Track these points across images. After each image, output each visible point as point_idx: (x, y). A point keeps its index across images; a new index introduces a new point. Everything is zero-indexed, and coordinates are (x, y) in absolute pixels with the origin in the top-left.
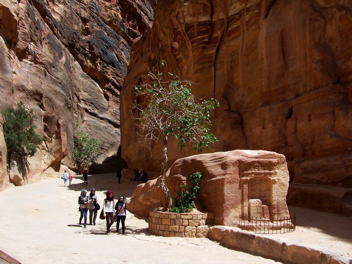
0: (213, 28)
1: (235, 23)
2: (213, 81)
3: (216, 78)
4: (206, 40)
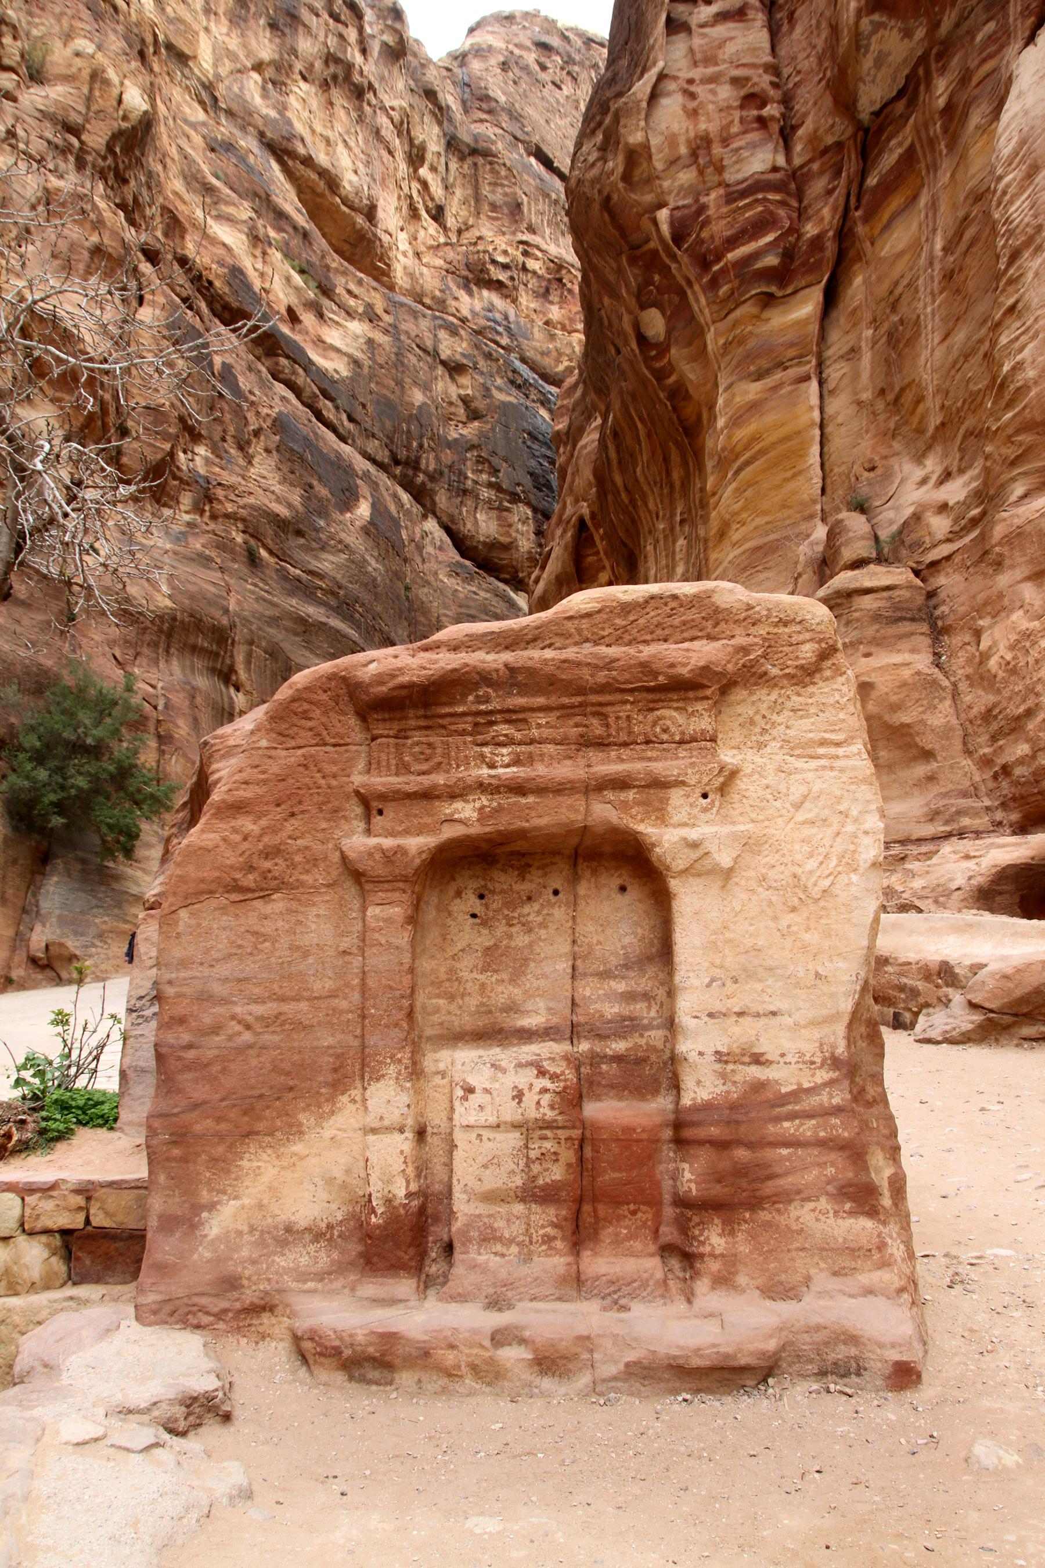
0: (800, 201)
1: (893, 142)
2: (815, 449)
3: (829, 429)
4: (771, 260)
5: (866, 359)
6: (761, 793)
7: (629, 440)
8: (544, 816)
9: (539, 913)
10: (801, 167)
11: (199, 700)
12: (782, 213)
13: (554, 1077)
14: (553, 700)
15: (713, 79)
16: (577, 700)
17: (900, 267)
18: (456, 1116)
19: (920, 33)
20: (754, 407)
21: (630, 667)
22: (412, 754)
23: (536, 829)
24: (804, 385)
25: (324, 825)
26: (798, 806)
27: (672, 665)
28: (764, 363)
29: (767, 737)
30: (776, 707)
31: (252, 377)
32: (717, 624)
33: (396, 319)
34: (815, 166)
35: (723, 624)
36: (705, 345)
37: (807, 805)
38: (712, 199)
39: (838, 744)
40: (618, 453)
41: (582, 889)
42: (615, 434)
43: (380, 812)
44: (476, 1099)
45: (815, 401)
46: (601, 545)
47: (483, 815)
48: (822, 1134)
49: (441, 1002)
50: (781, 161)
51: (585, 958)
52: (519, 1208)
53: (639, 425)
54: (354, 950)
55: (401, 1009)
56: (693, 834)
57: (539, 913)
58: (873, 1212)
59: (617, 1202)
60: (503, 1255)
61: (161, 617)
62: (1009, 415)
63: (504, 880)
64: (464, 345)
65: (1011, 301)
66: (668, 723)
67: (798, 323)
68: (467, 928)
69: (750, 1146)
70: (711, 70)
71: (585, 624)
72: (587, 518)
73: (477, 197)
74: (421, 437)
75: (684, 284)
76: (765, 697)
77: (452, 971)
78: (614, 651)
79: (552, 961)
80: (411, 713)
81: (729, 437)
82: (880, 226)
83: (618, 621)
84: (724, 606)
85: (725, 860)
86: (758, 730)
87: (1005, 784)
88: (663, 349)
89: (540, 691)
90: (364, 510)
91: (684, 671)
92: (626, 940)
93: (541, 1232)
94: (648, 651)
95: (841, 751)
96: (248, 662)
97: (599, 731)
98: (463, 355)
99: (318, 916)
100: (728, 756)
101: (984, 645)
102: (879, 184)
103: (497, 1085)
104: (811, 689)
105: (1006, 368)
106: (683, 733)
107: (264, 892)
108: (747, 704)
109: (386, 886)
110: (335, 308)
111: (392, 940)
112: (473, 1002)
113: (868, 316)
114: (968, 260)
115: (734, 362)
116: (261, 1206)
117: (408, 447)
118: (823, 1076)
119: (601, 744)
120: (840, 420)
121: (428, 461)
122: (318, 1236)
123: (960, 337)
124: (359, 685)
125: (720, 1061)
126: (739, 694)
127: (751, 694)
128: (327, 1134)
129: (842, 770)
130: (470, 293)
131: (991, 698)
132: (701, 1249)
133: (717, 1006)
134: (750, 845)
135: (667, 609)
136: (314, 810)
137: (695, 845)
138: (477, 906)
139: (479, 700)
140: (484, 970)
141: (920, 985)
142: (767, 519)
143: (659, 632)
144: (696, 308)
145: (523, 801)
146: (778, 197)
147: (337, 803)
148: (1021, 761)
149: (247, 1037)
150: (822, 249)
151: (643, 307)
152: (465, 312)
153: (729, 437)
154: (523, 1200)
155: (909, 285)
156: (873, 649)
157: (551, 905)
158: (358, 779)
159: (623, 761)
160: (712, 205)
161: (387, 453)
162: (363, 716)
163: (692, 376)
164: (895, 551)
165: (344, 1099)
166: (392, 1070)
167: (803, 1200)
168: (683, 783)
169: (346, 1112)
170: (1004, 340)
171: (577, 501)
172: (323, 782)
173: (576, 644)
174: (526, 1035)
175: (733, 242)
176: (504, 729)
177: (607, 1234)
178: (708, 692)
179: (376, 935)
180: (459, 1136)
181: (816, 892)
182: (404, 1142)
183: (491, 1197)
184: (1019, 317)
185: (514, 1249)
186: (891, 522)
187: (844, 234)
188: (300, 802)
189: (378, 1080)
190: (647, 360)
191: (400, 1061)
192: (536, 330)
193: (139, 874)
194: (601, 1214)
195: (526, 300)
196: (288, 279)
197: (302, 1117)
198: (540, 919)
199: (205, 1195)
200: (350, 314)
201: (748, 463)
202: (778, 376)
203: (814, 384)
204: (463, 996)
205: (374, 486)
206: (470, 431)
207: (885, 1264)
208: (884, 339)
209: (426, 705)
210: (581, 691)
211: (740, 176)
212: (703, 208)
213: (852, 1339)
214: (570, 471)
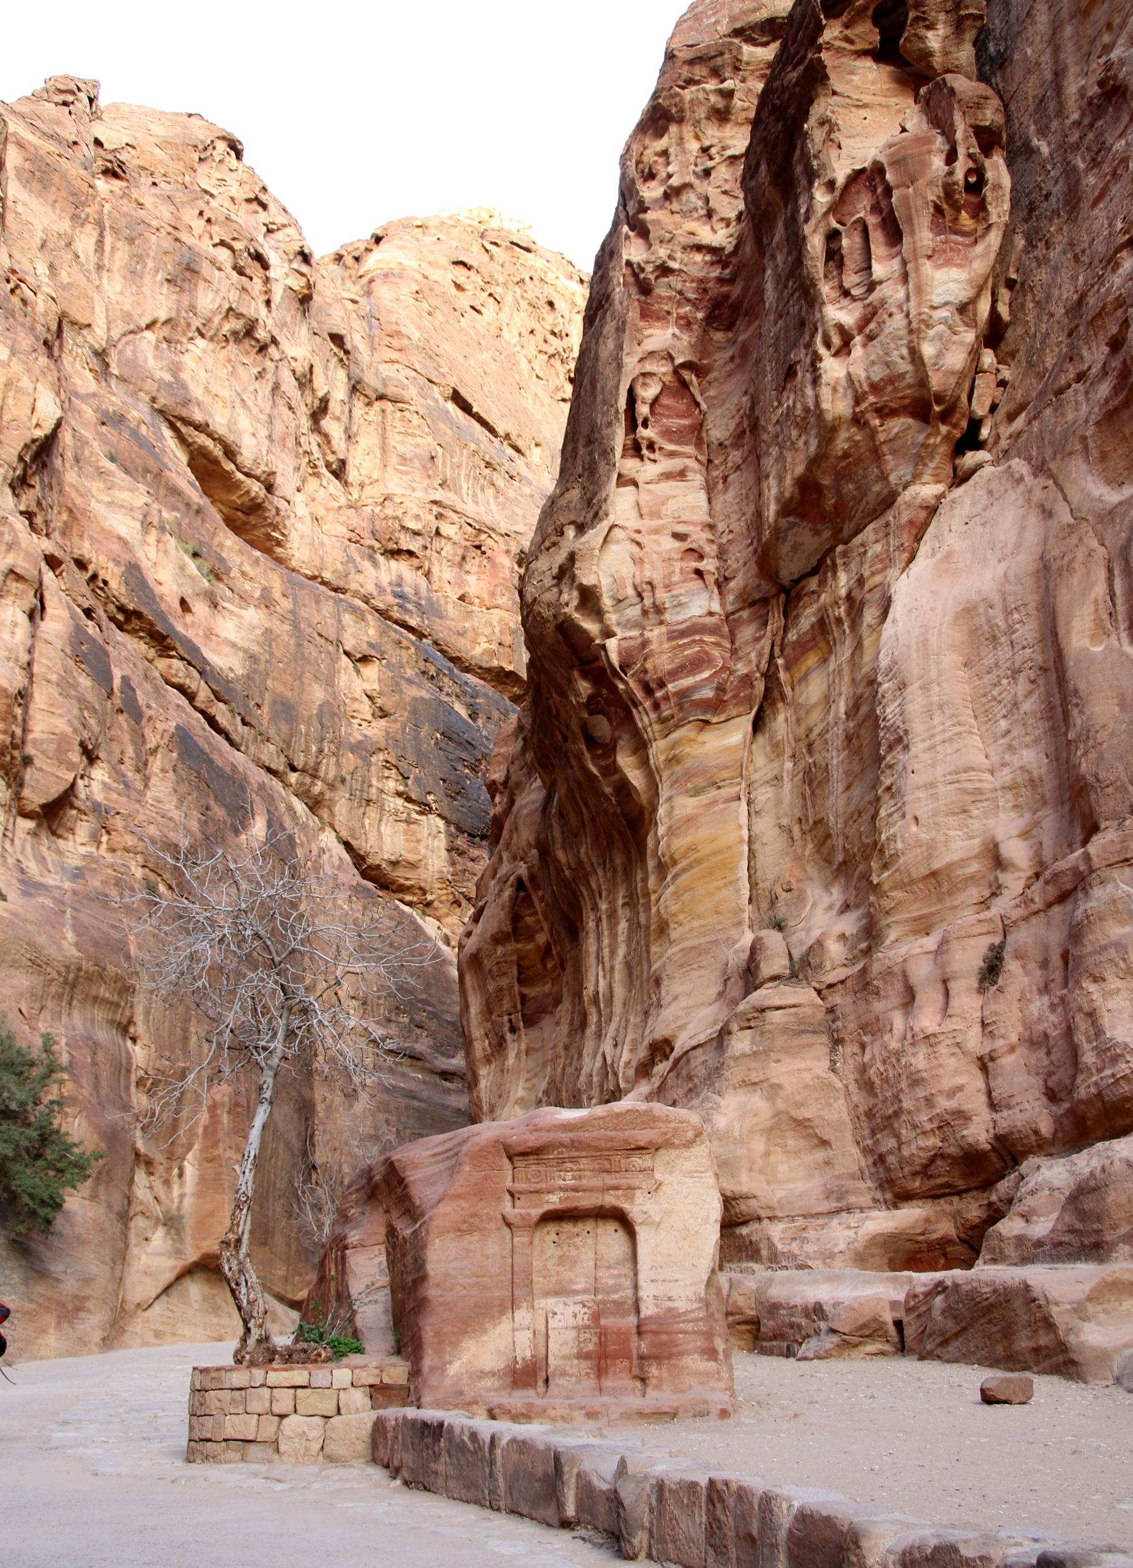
1: (808, 610)
2: (744, 864)
3: (755, 846)
4: (708, 693)
5: (787, 786)
7: (573, 821)
8: (587, 1201)
10: (733, 613)
11: (100, 1056)
12: (716, 653)
15: (656, 531)
17: (815, 717)
19: (827, 534)
20: (690, 820)
24: (735, 804)
28: (700, 782)
30: (678, 1157)
31: (148, 686)
33: (295, 602)
34: (745, 614)
36: (648, 759)
38: (655, 634)
40: (563, 832)
41: (600, 1231)
42: (561, 814)
45: (744, 820)
46: (539, 906)
47: (561, 1200)
50: (716, 607)
52: (575, 1362)
53: (584, 810)
58: (716, 1360)
59: (615, 1358)
61: (68, 968)
62: (886, 874)
63: (567, 1227)
64: (371, 632)
65: (888, 782)
67: (728, 749)
69: (667, 1333)
70: (655, 523)
72: (525, 878)
73: (384, 450)
74: (322, 740)
76: (674, 1153)
78: (613, 1133)
81: (668, 846)
82: (797, 676)
85: (657, 1219)
87: (881, 1170)
89: (584, 1150)
90: (259, 828)
91: (642, 1144)
94: (627, 1133)
96: (147, 1013)
98: (370, 645)
100: (658, 1176)
101: (868, 1056)
102: (797, 642)
105: (883, 837)
107: (470, 1232)
110: (229, 593)
112: (554, 1279)
113: (788, 751)
116: (470, 1362)
117: (306, 751)
118: (695, 1306)
119: (607, 1171)
120: (764, 840)
121: (329, 769)
122: (494, 1375)
123: (856, 792)
126: (662, 1151)
130: (375, 564)
131: (872, 1101)
134: (668, 1213)
138: (555, 1238)
141: (804, 1322)
142: (702, 922)
144: (640, 725)
146: (713, 639)
148: (890, 1152)
149: (464, 1292)
150: (752, 687)
151: (591, 713)
152: (370, 588)
153: (668, 846)
156: (781, 1056)
158: (509, 1184)
160: (655, 640)
161: (283, 759)
162: (510, 1158)
163: (635, 783)
164: (802, 968)
166: (525, 1305)
170: (883, 813)
171: (514, 858)
174: (576, 1292)
175: (675, 674)
176: (569, 1165)
177: (611, 1370)
182: (529, 1334)
183: (564, 1357)
186: (802, 943)
187: (770, 676)
190: (595, 758)
192: (450, 606)
193: (42, 1248)
195: (443, 572)
196: (182, 568)
199: (447, 1358)
200: (244, 599)
201: (684, 870)
202: (713, 793)
203: (744, 803)
205: (270, 800)
206: (376, 730)
207: (720, 1379)
208: (801, 775)
210: (600, 1150)
211: (680, 618)
212: (645, 643)
213: (706, 1402)
214: (507, 825)
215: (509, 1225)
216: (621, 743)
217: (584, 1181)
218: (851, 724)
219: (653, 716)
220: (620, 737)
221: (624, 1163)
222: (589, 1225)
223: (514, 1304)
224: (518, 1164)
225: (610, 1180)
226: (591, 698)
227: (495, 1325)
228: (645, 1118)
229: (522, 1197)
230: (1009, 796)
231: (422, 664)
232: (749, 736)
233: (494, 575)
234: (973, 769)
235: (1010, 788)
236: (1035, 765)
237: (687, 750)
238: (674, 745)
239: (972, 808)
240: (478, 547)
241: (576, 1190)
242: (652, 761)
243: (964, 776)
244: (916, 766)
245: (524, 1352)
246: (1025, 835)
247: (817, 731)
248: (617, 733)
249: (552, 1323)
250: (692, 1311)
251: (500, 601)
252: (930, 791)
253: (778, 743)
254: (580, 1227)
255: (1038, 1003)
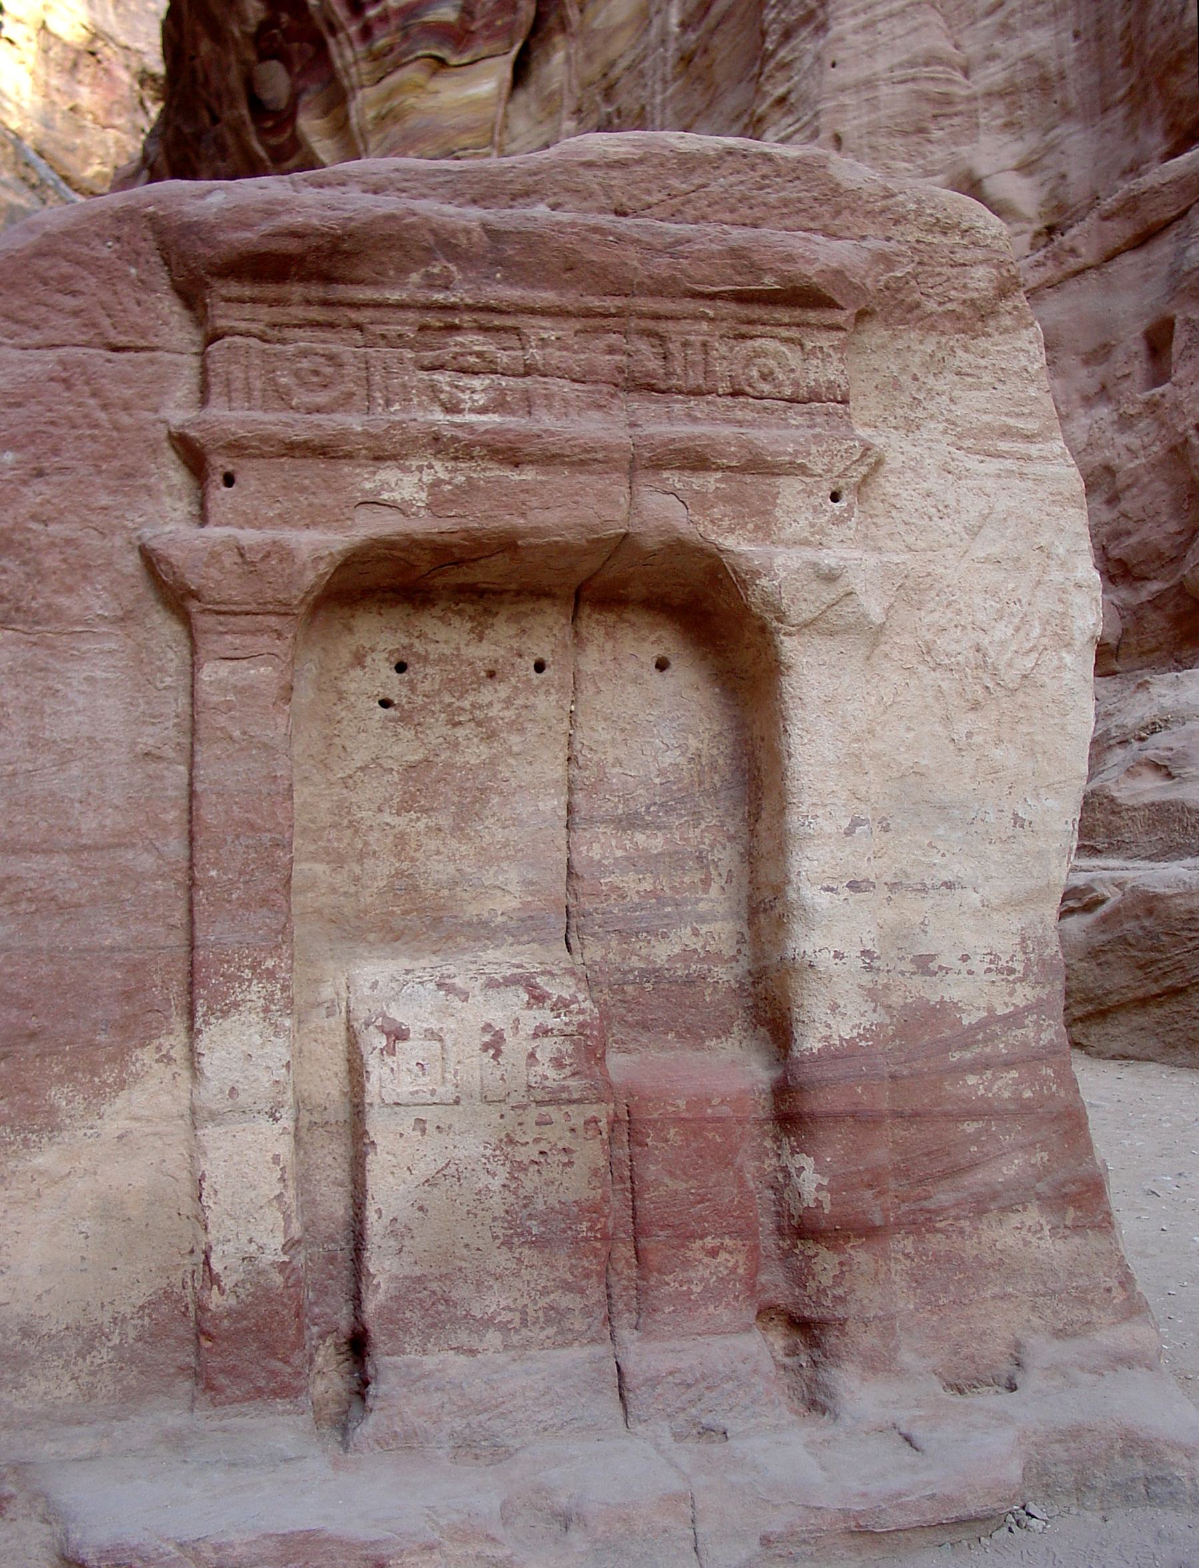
6: (919, 503)
8: (558, 510)
9: (508, 703)
13: (561, 1006)
14: (570, 299)
16: (612, 303)
17: (620, 44)
18: (372, 1086)
21: (712, 255)
22: (297, 374)
23: (536, 531)
25: (105, 500)
26: (974, 532)
27: (790, 259)
29: (920, 413)
30: (935, 364)
32: (837, 213)
35: (846, 213)
36: (347, 118)
37: (988, 532)
39: (1028, 438)
41: (591, 661)
43: (229, 480)
44: (413, 1049)
47: (437, 503)
48: (1028, 1094)
49: (320, 868)
51: (592, 790)
54: (169, 752)
55: (273, 867)
56: (829, 559)
57: (508, 703)
60: (472, 1352)
63: (446, 637)
65: (780, 91)
66: (772, 363)
67: (473, 102)
68: (374, 725)
71: (617, 178)
75: (324, 28)
76: (920, 345)
77: (343, 807)
79: (533, 795)
80: (296, 290)
83: (675, 182)
84: (847, 185)
85: (876, 613)
86: (905, 399)
88: (287, 117)
89: (550, 280)
91: (810, 272)
92: (668, 759)
93: (543, 1302)
95: (1033, 450)
97: (654, 364)
99: (90, 680)
103: (451, 1024)
104: (983, 343)
106: (796, 384)
108: (885, 353)
109: (243, 621)
111: (254, 730)
112: (382, 869)
113: (569, 104)
114: (716, 40)
115: (387, 144)
124: (190, 229)
125: (869, 968)
126: (875, 334)
127: (894, 337)
128: (112, 1126)
129: (1038, 480)
132: (840, 1312)
133: (866, 870)
135: (756, 176)
136: (84, 470)
137: (830, 577)
138: (394, 687)
139: (431, 282)
140: (404, 808)
143: (745, 211)
144: (338, 63)
145: (515, 476)
147: (130, 460)
151: (263, 57)
154: (507, 1243)
155: (628, 68)
157: (534, 691)
158: (178, 411)
159: (695, 420)
162: (191, 295)
165: (146, 1055)
166: (255, 992)
167: (1003, 1209)
168: (803, 470)
169: (151, 1084)
172: (102, 416)
173: (602, 210)
174: (484, 932)
178: (840, 317)
179: (222, 720)
180: (378, 1125)
181: (1011, 677)
184: (790, 112)
185: (493, 1338)
188: (56, 451)
189: (225, 1014)
190: (262, 133)
191: (271, 974)
194: (654, 1259)
197: (58, 1095)
198: (509, 714)
204: (361, 858)
209: (327, 279)
215: (172, 592)
216: (305, 98)
217: (545, 421)
218: (693, 37)
219: (361, 49)
220: (304, 90)
221: (728, 360)
222: (545, 633)
223: (196, 990)
224: (225, 316)
225: (665, 423)
226: (264, 26)
227: (99, 1094)
228: (791, 192)
229: (250, 474)
230: (999, 107)
231: (21, 168)
232: (507, 84)
233: (112, 90)
234: (940, 61)
235: (1001, 95)
236: (1052, 53)
237: (411, 101)
238: (391, 93)
239: (931, 126)
240: (93, 54)
241: (509, 453)
242: (354, 120)
243: (925, 71)
244: (841, 55)
245: (254, 1218)
246: (1026, 167)
247: (623, 63)
248: (301, 83)
249: (386, 1079)
250: (1014, 1019)
251: (119, 121)
252: (866, 95)
253: (550, 98)
254: (500, 641)
255: (1085, 421)
